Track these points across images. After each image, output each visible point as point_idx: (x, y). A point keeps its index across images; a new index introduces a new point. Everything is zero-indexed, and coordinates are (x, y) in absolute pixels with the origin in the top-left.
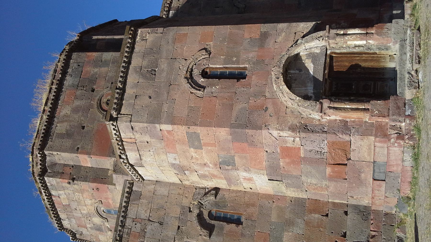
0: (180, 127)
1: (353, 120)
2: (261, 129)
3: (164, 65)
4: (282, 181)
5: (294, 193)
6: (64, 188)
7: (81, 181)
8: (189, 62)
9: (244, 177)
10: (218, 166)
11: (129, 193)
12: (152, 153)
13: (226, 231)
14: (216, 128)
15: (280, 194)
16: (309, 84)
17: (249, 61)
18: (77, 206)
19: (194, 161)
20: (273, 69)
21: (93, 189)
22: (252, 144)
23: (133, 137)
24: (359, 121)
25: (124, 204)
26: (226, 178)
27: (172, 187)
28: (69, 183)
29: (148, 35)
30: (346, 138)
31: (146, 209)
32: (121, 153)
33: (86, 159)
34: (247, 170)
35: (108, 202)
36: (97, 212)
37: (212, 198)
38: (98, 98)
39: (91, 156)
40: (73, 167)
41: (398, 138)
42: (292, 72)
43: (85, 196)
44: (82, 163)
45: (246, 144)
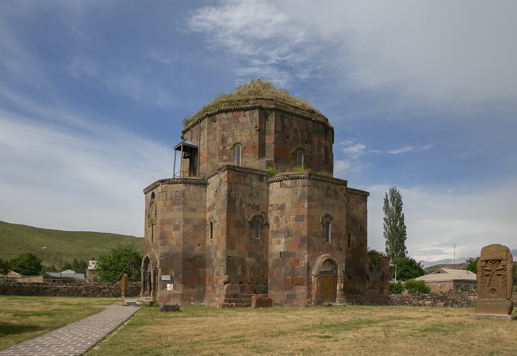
0: (307, 212)
1: (312, 286)
2: (308, 250)
3: (331, 201)
4: (280, 257)
5: (272, 262)
6: (252, 122)
7: (259, 136)
8: (332, 214)
9: (280, 240)
10: (286, 229)
11: (262, 175)
12: (291, 194)
13: (252, 230)
14: (307, 230)
15: (269, 256)
16: (323, 269)
17: (332, 243)
18: (239, 128)
19: (288, 216)
20: (330, 254)
21: (254, 144)
22: (300, 246)
23: (299, 185)
24: (312, 289)
25: (258, 172)
26: (277, 231)
27: (267, 199)
28: (256, 127)
29: (343, 192)
30: (306, 284)
31: (256, 185)
32: (290, 177)
33: (271, 140)
34: (286, 242)
35: (245, 153)
36: (237, 142)
37: (265, 223)
38: (302, 146)
39: (273, 145)
40: (265, 129)
41: (308, 302)
42: (328, 262)
43: (248, 136)
44: (268, 136)
45: (299, 243)
